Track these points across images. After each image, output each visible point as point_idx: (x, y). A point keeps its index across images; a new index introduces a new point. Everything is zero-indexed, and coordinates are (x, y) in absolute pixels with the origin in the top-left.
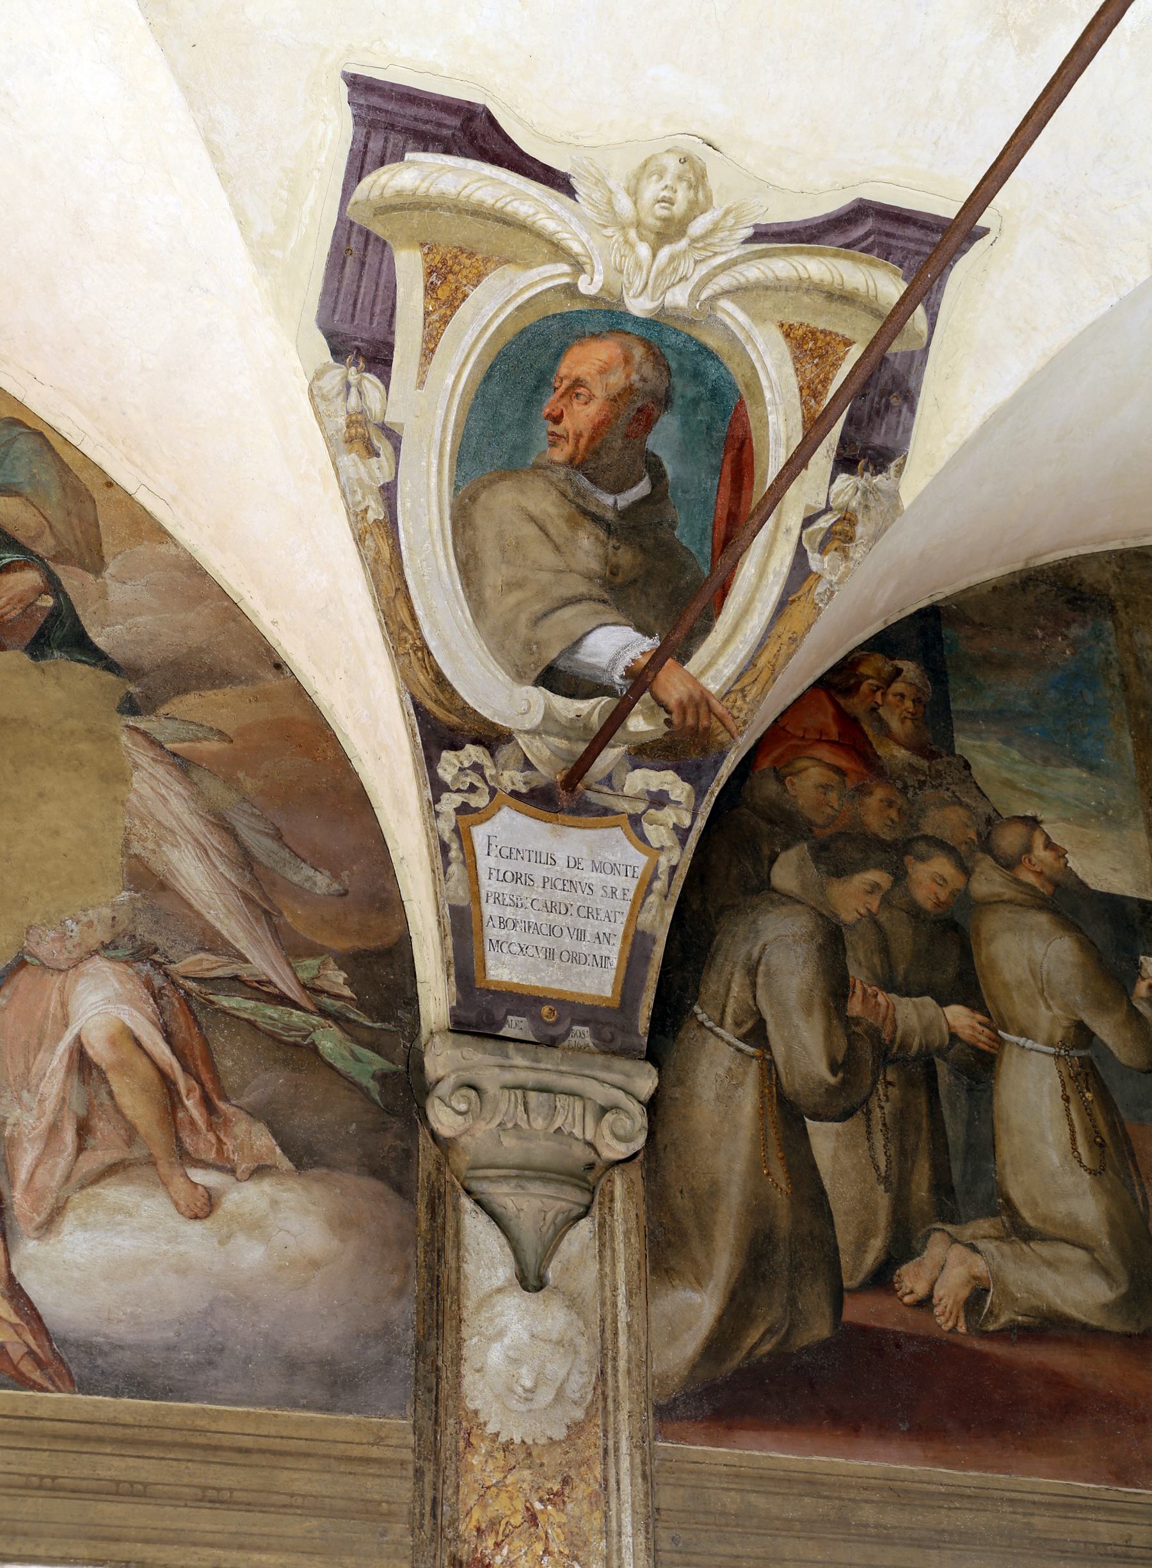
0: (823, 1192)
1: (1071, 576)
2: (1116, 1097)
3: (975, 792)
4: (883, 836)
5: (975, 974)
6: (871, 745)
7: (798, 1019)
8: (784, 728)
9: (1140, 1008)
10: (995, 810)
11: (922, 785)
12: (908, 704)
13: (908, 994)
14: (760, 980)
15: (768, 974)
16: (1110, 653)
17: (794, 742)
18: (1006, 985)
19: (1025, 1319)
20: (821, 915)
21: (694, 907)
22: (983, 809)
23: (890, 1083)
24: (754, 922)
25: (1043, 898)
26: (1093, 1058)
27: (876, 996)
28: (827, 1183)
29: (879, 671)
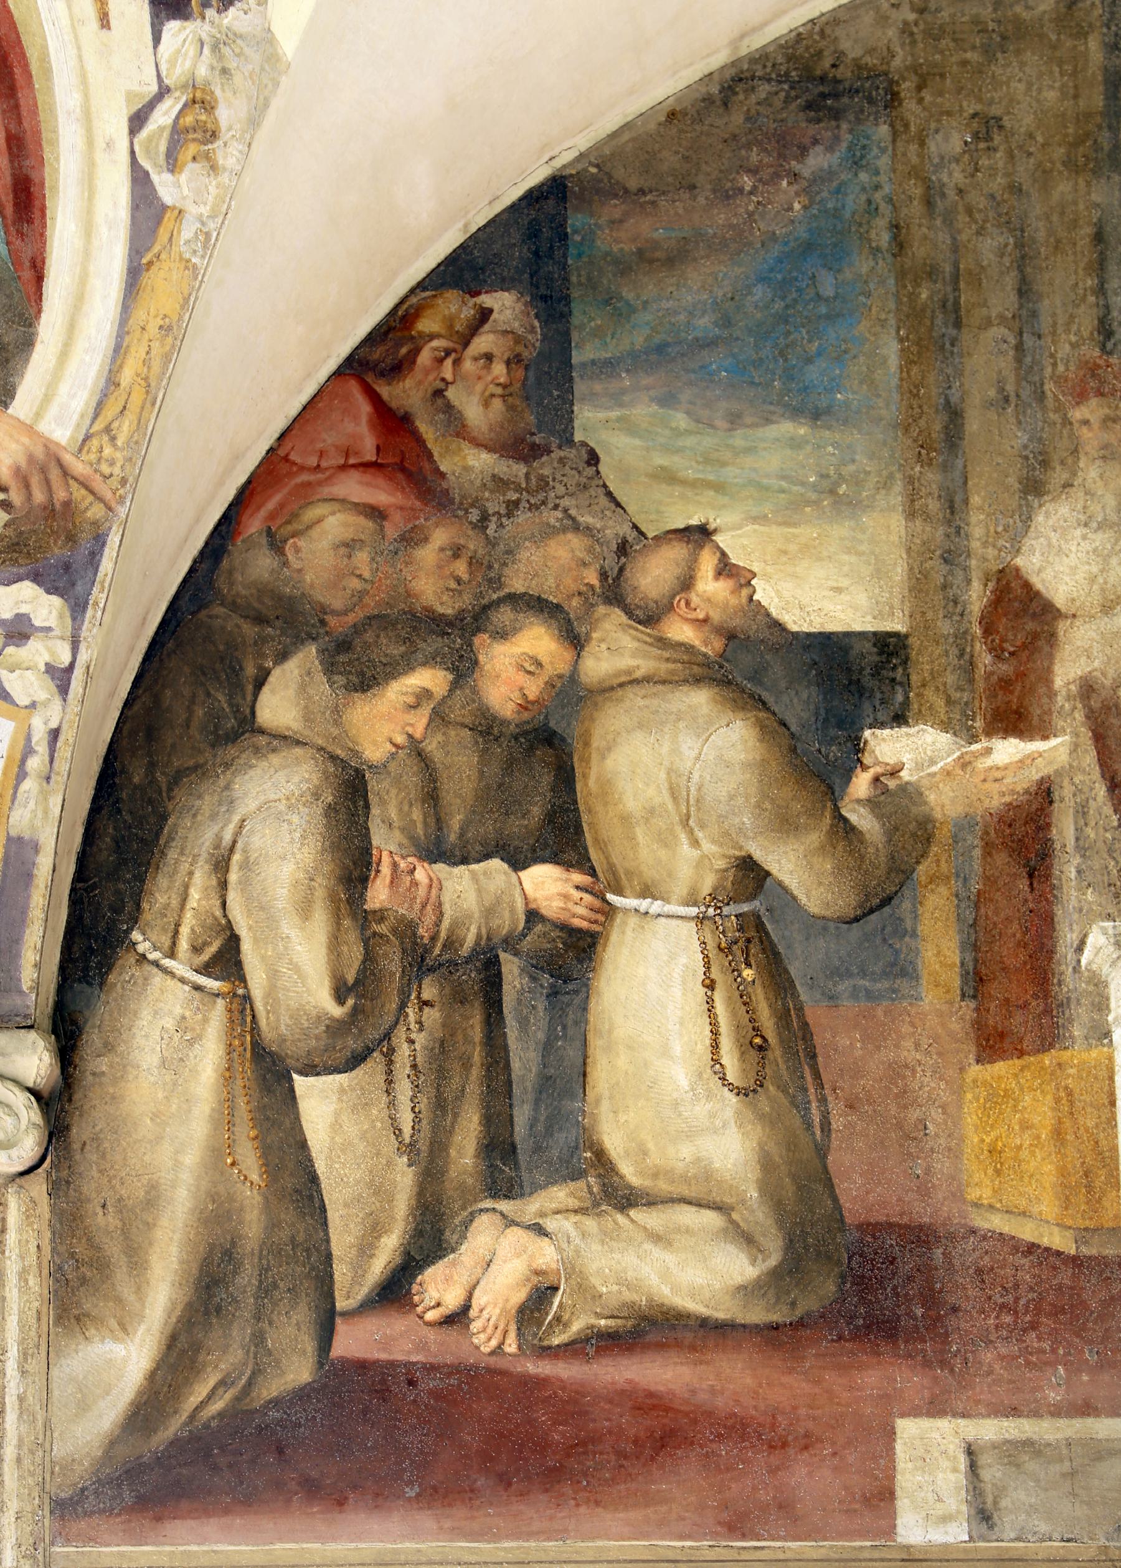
0: (314, 1179)
1: (819, 53)
2: (795, 970)
3: (604, 501)
4: (441, 610)
5: (577, 810)
6: (430, 455)
7: (289, 927)
8: (286, 459)
9: (853, 818)
10: (635, 527)
11: (512, 507)
12: (499, 370)
13: (465, 861)
14: (233, 877)
15: (245, 865)
16: (877, 187)
17: (304, 477)
18: (626, 819)
19: (611, 1322)
20: (333, 758)
21: (136, 780)
22: (615, 529)
23: (426, 1003)
24: (227, 787)
25: (706, 663)
26: (762, 912)
27: (412, 871)
28: (321, 1167)
29: (450, 322)
